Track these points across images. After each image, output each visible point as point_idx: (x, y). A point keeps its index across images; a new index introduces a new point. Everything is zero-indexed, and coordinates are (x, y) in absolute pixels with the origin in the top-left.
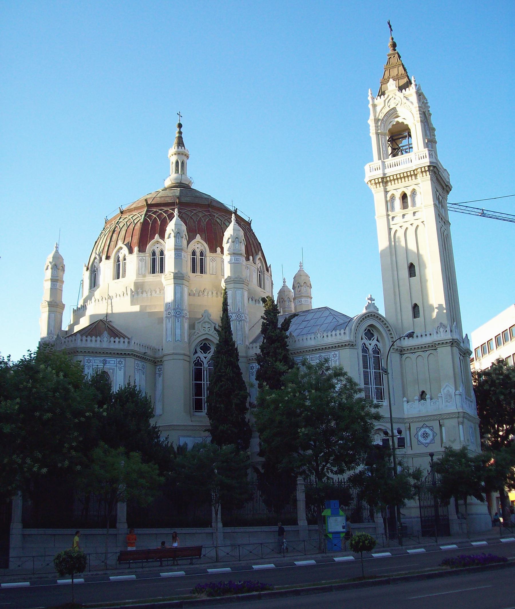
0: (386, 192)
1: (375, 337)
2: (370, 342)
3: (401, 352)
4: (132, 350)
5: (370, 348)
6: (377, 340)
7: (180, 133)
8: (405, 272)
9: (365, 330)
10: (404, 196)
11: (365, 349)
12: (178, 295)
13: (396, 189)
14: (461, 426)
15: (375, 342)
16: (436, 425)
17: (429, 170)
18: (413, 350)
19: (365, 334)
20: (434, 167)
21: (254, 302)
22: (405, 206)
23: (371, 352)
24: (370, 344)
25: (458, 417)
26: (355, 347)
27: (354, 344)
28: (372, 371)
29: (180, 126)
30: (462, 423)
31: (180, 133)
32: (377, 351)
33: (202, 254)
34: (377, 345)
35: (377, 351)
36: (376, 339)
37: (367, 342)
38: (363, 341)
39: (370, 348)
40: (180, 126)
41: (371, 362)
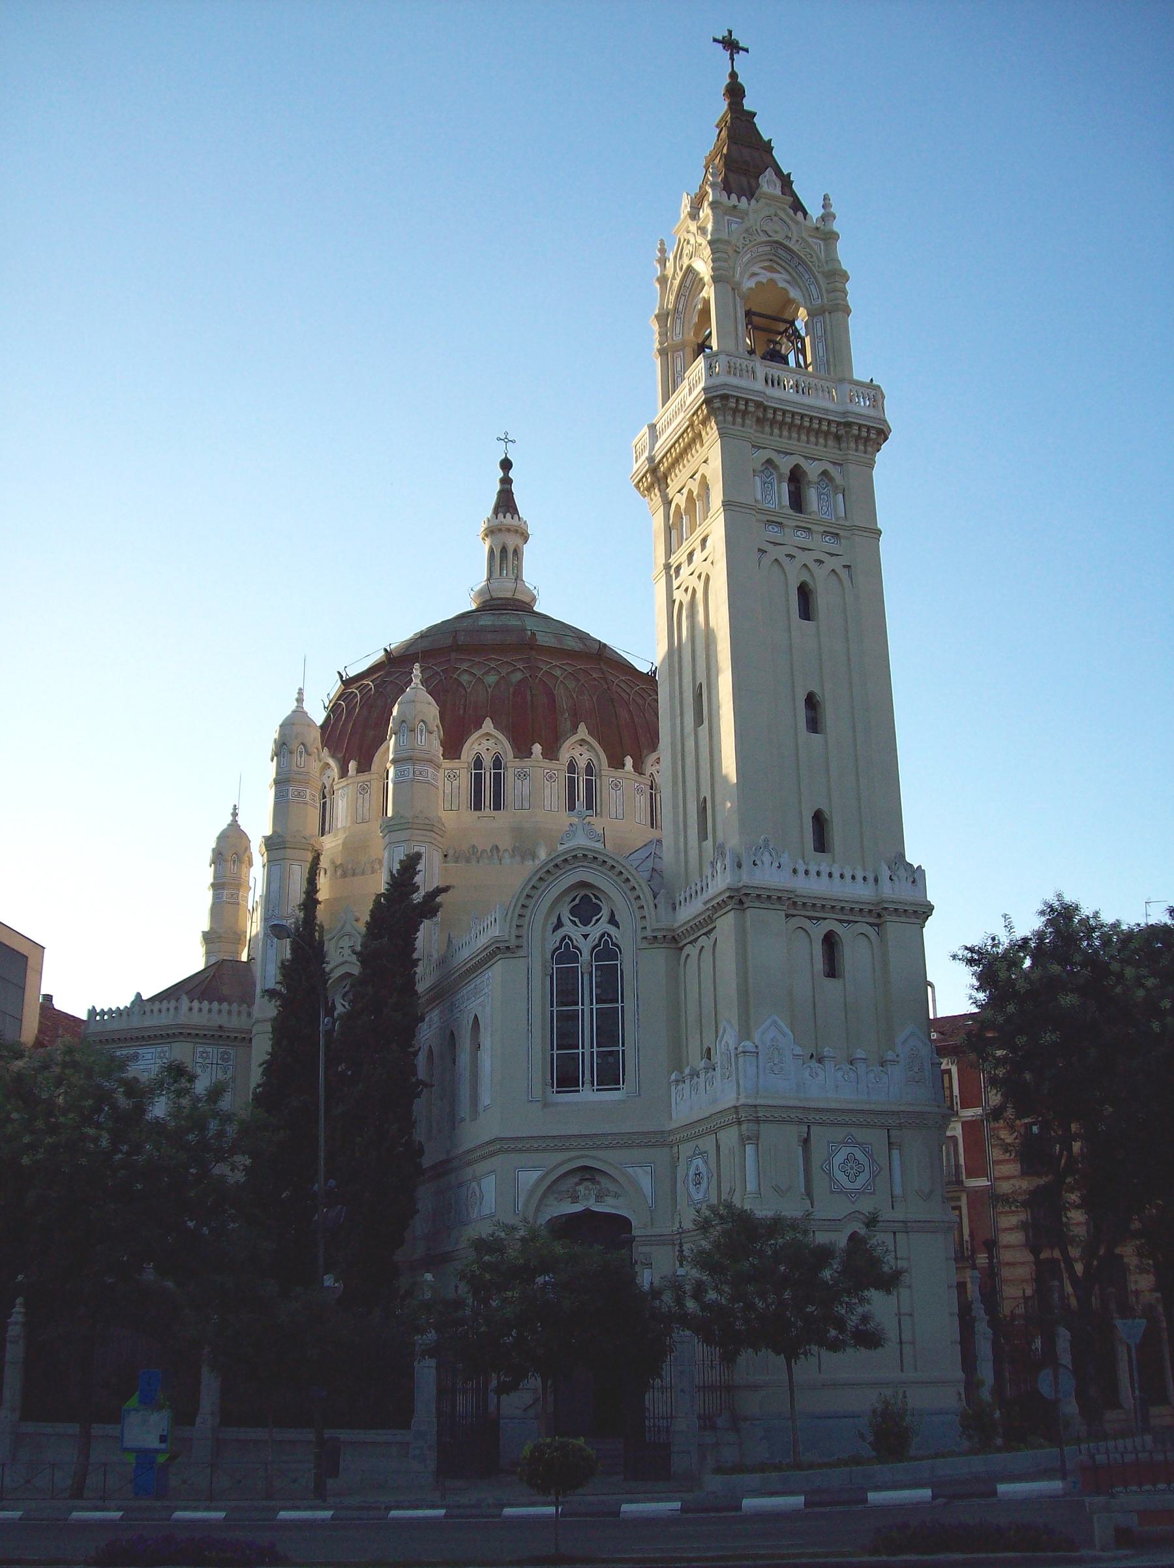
0: (667, 503)
1: (605, 913)
2: (587, 929)
3: (673, 941)
4: (178, 1026)
5: (585, 947)
6: (613, 921)
7: (506, 481)
9: (573, 900)
11: (566, 953)
12: (275, 886)
14: (749, 1149)
17: (712, 412)
19: (572, 912)
20: (725, 397)
21: (518, 858)
23: (585, 956)
24: (586, 936)
25: (739, 1123)
26: (521, 953)
27: (513, 943)
28: (587, 1008)
29: (506, 465)
30: (755, 1139)
31: (506, 481)
34: (609, 936)
35: (606, 951)
36: (605, 919)
37: (573, 931)
38: (561, 932)
39: (585, 947)
40: (506, 465)
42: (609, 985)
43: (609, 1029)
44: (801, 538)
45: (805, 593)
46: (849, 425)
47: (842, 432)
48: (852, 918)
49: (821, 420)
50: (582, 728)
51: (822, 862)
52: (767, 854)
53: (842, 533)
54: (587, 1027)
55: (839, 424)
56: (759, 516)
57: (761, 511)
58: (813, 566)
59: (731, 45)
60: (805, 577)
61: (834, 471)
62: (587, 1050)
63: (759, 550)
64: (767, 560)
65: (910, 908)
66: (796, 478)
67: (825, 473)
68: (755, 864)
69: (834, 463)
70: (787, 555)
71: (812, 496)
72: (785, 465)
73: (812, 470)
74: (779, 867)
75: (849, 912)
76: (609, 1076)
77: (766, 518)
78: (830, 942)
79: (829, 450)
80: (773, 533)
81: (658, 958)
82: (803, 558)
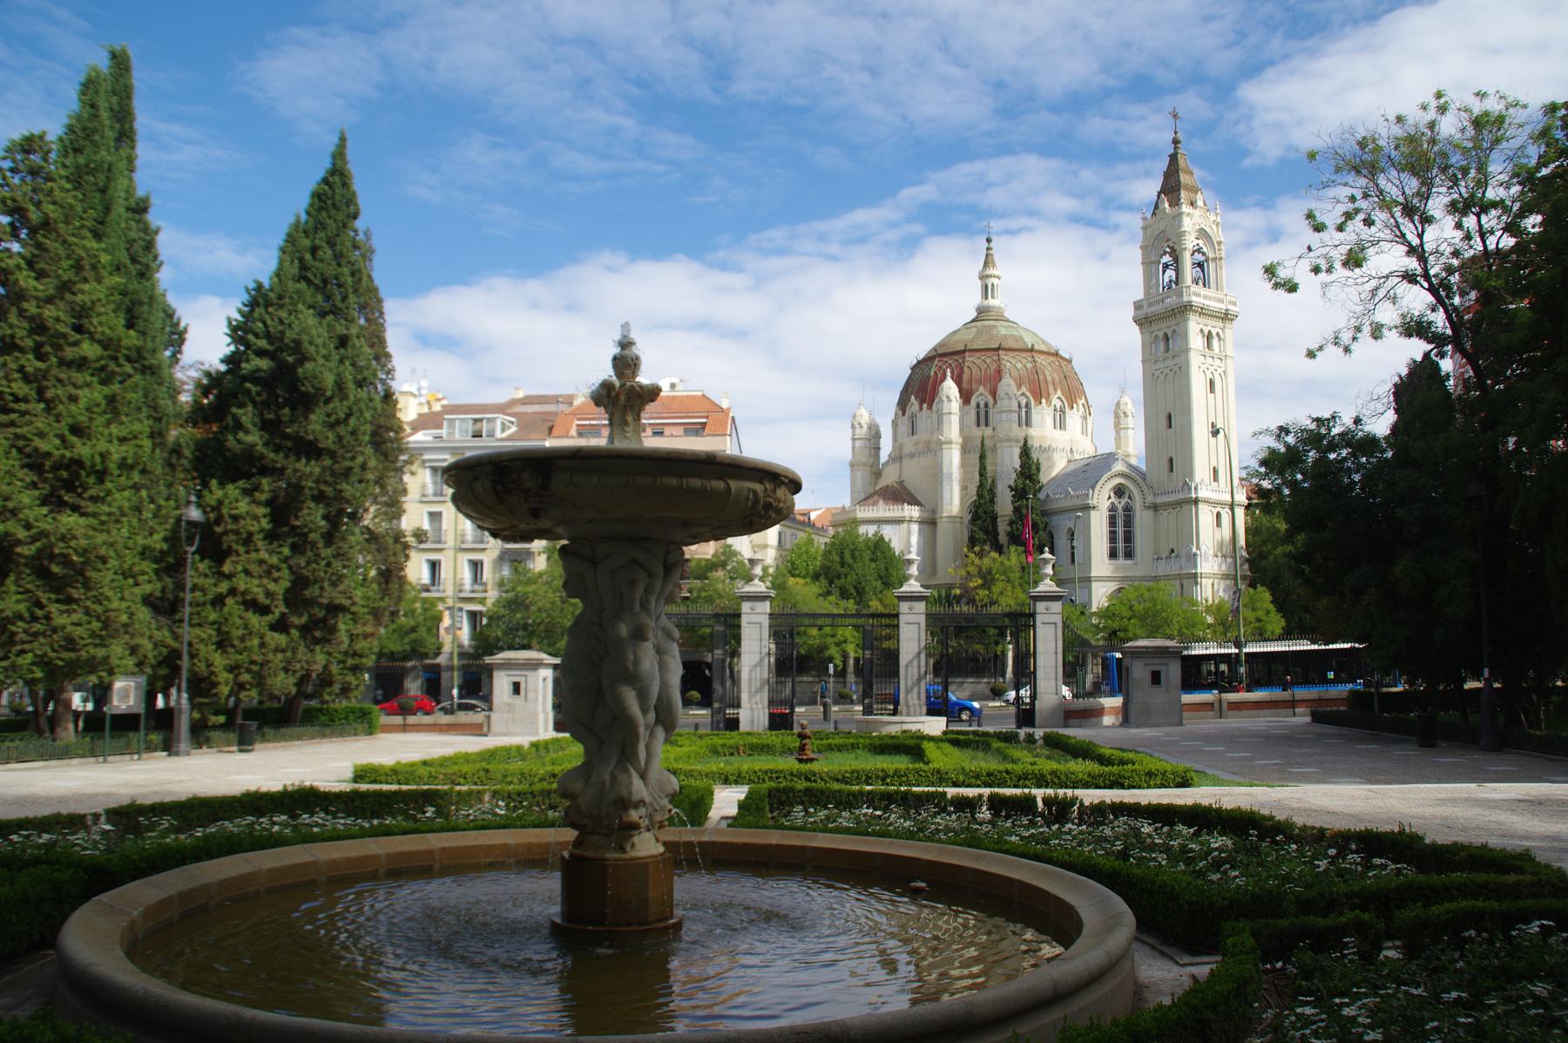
3: (1155, 508)
5: (1120, 507)
8: (1164, 422)
10: (1166, 338)
11: (1113, 509)
13: (1159, 329)
15: (1124, 500)
16: (1177, 583)
18: (1166, 505)
22: (1167, 350)
28: (1120, 530)
29: (989, 241)
32: (1128, 509)
33: (986, 405)
35: (1128, 509)
41: (1120, 522)
42: (1128, 522)
43: (1128, 538)
50: (1059, 393)
54: (1120, 536)
59: (1175, 116)
62: (1121, 545)
71: (1215, 341)
76: (1129, 554)
78: (1218, 515)
79: (1220, 324)
81: (1150, 513)
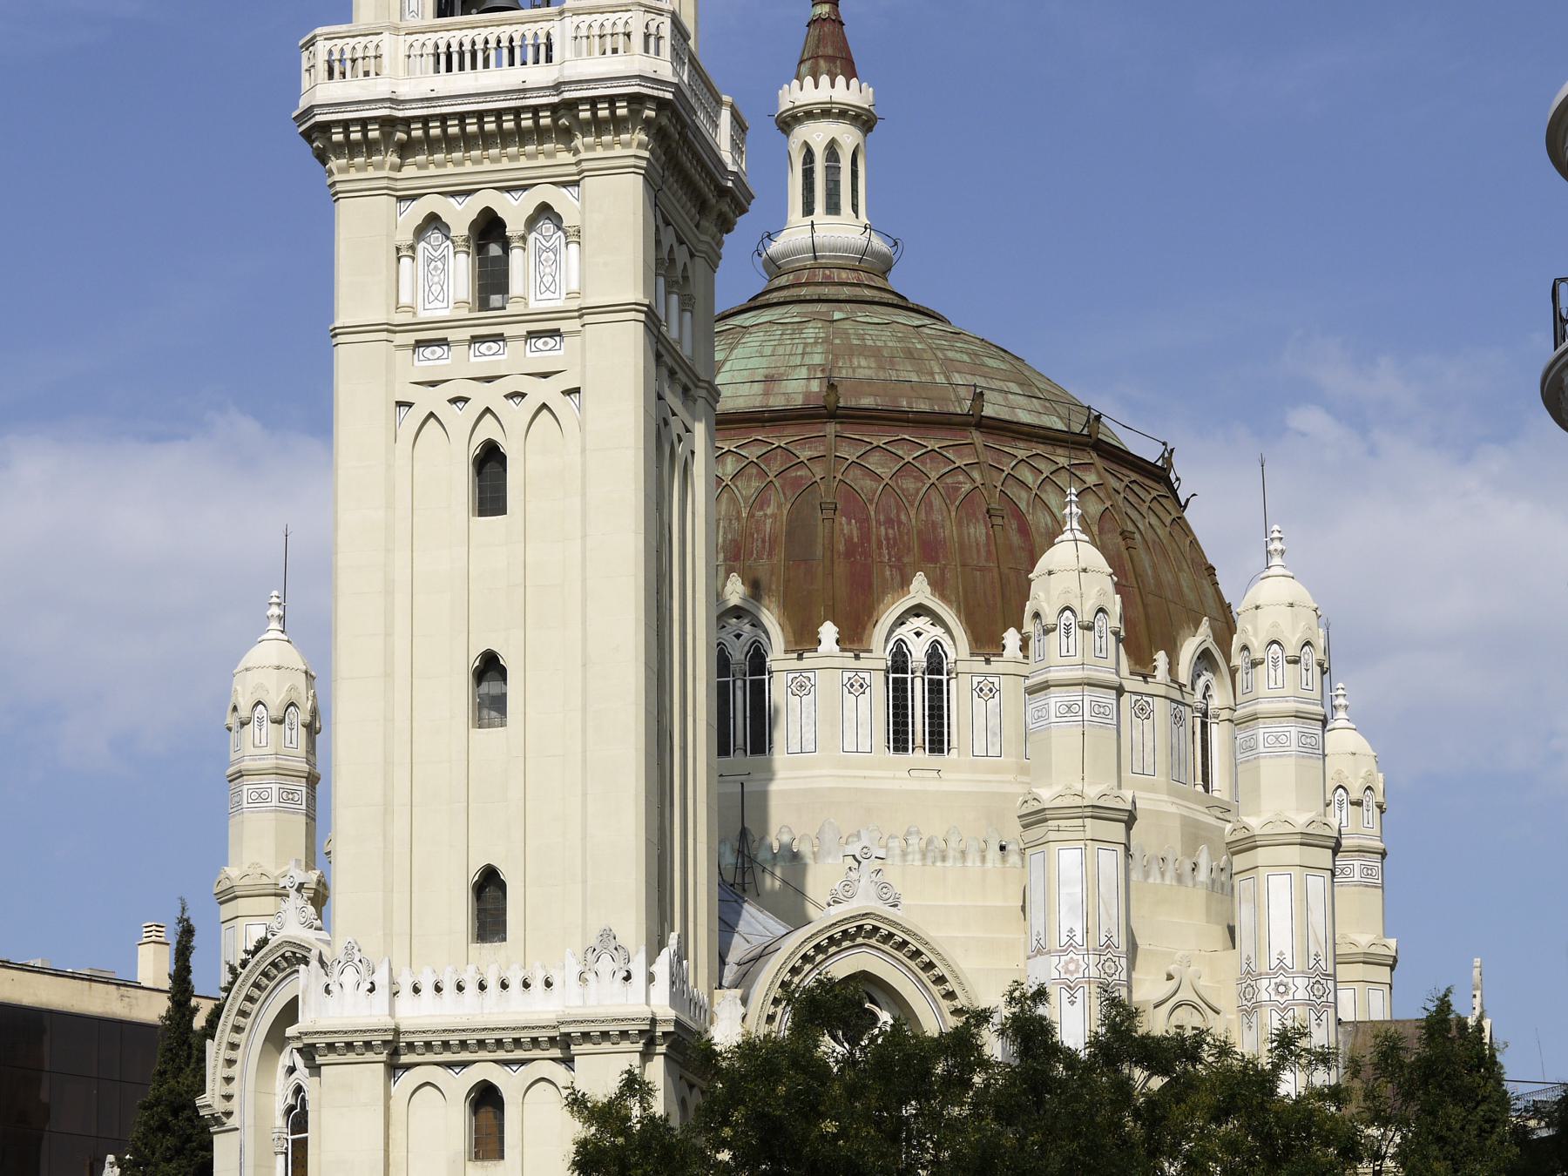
44: (487, 358)
45: (490, 460)
46: (571, 105)
47: (564, 121)
48: (519, 1054)
49: (517, 112)
51: (492, 959)
52: (350, 971)
53: (564, 326)
55: (554, 108)
56: (400, 339)
57: (392, 328)
58: (504, 408)
60: (488, 430)
61: (562, 200)
63: (400, 404)
64: (414, 417)
65: (614, 1028)
66: (489, 228)
67: (544, 211)
68: (328, 991)
69: (565, 185)
70: (454, 401)
72: (461, 215)
73: (514, 211)
74: (372, 990)
75: (515, 1046)
77: (411, 338)
80: (432, 362)
82: (484, 396)
